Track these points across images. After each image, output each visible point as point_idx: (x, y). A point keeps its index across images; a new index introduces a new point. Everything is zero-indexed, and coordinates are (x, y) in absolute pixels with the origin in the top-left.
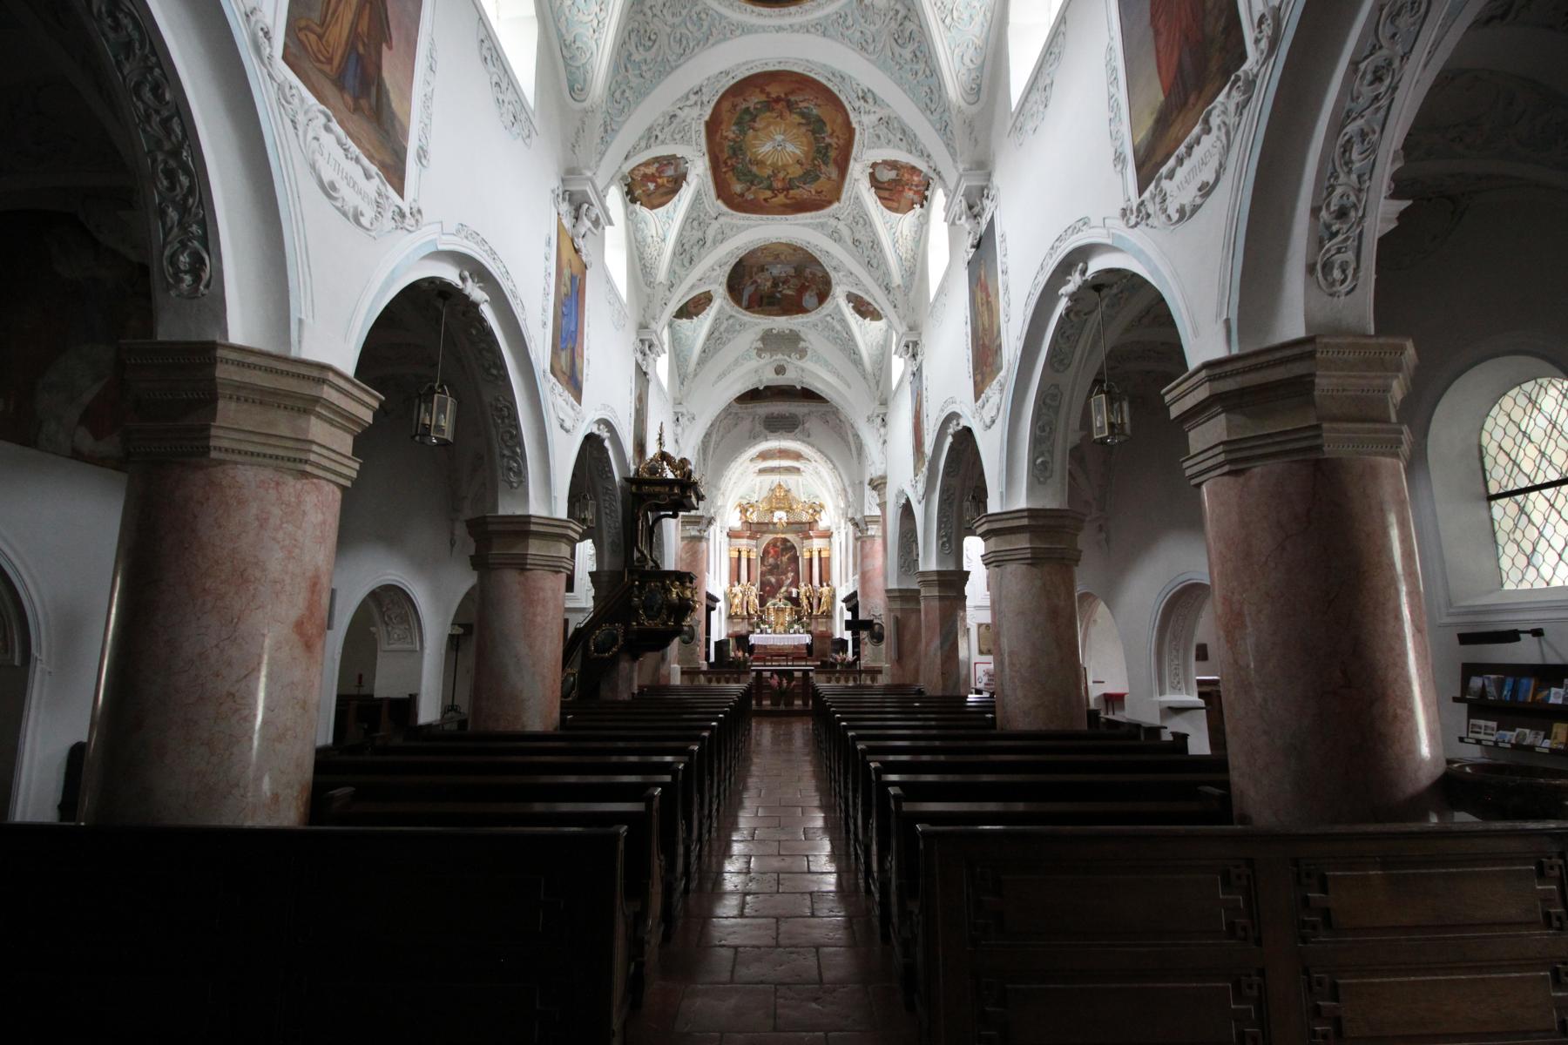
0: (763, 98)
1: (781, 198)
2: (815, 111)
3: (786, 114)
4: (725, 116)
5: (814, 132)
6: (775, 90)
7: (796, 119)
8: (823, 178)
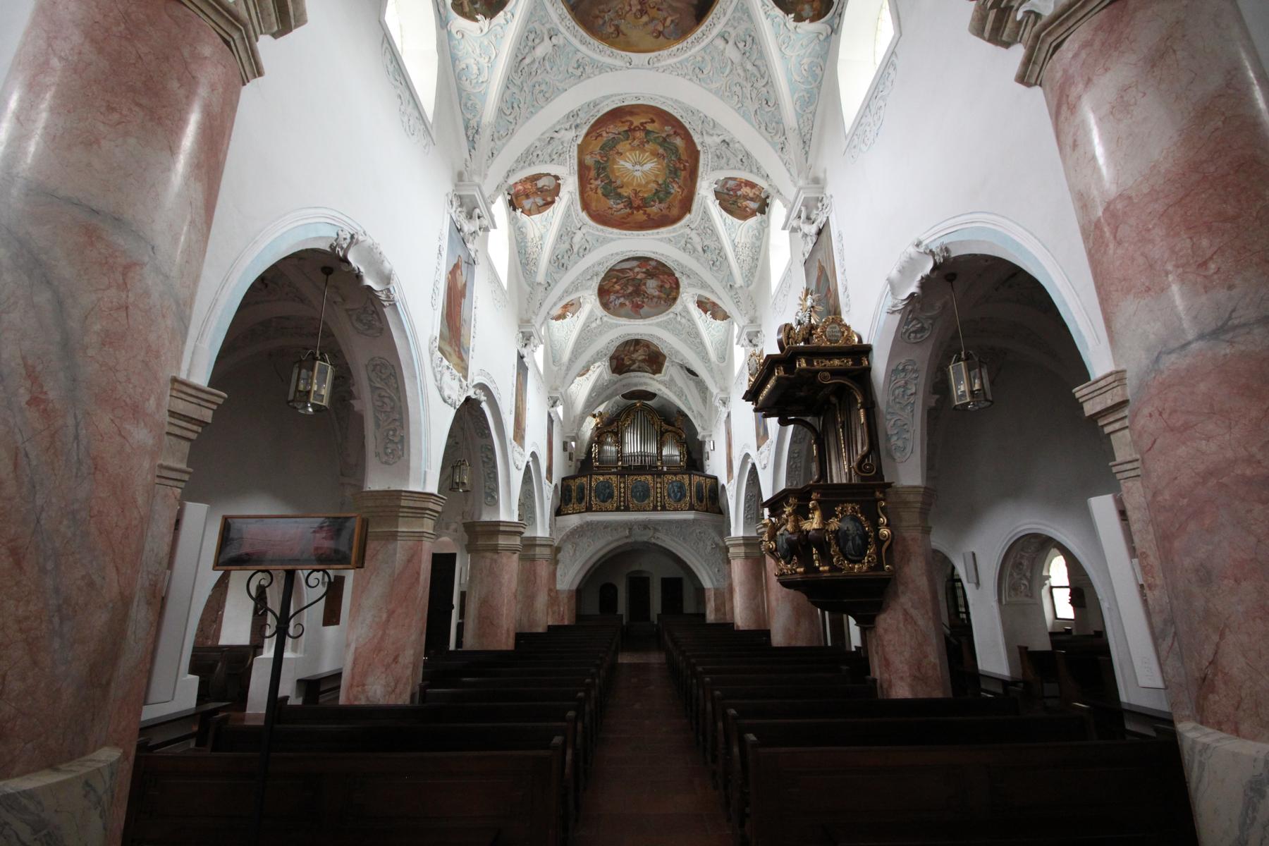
0: (648, 210)
1: (637, 121)
2: (611, 202)
3: (632, 195)
4: (676, 203)
5: (611, 182)
6: (640, 216)
7: (625, 192)
8: (597, 150)
